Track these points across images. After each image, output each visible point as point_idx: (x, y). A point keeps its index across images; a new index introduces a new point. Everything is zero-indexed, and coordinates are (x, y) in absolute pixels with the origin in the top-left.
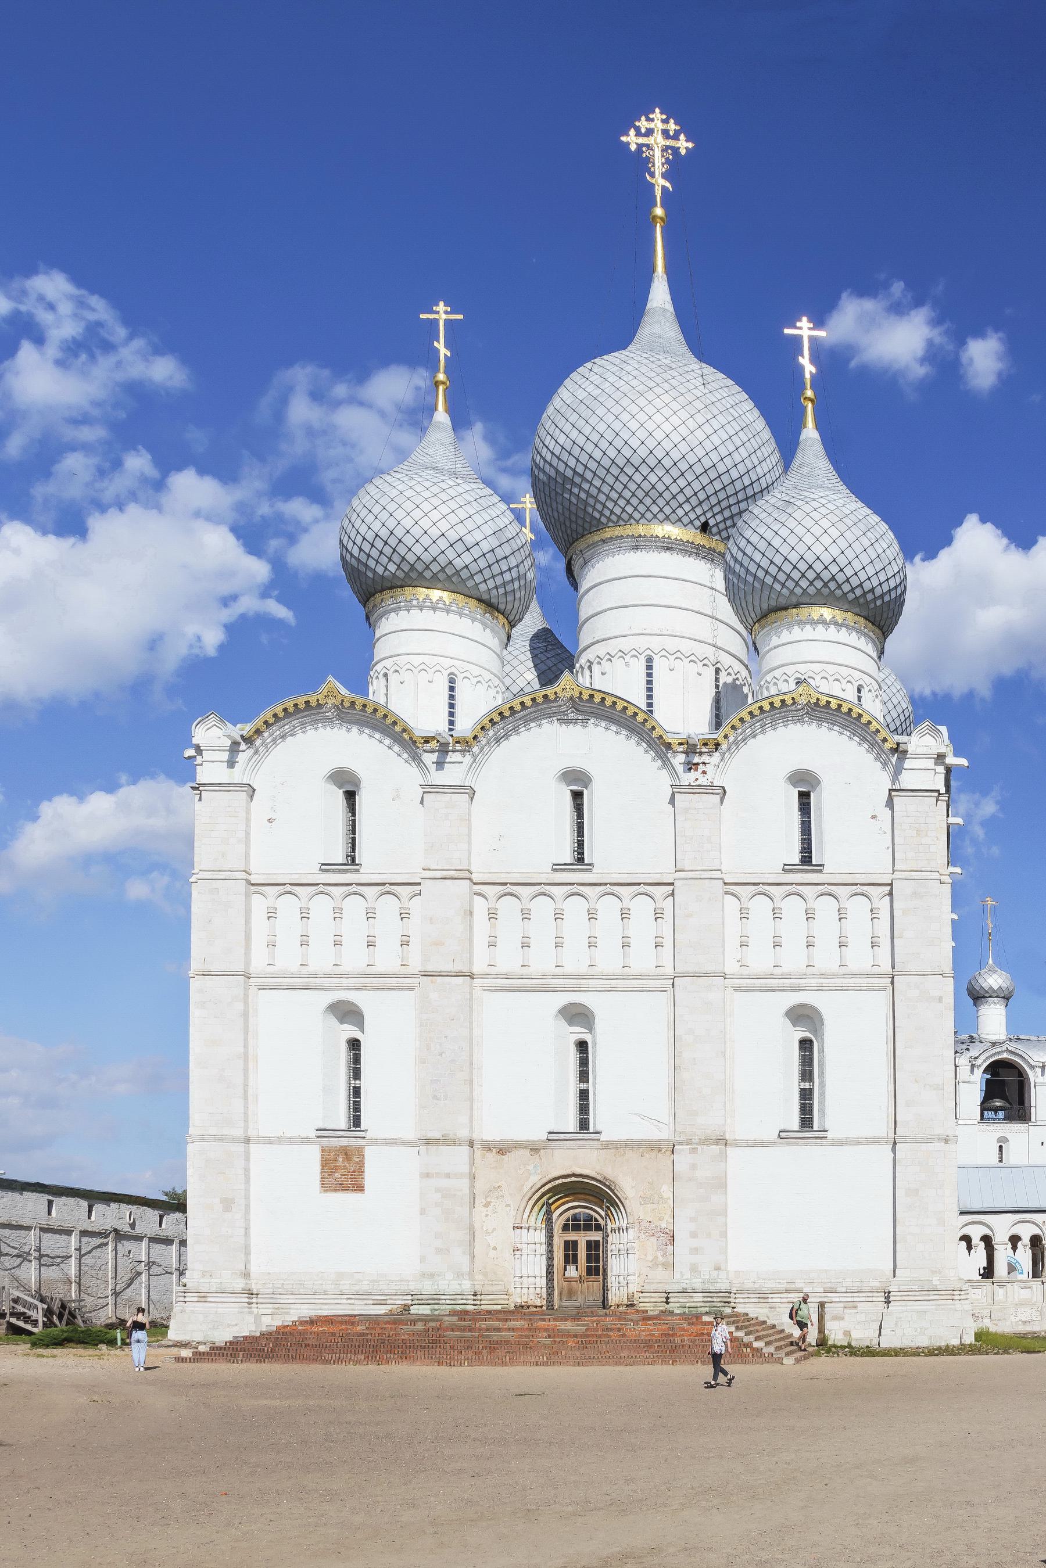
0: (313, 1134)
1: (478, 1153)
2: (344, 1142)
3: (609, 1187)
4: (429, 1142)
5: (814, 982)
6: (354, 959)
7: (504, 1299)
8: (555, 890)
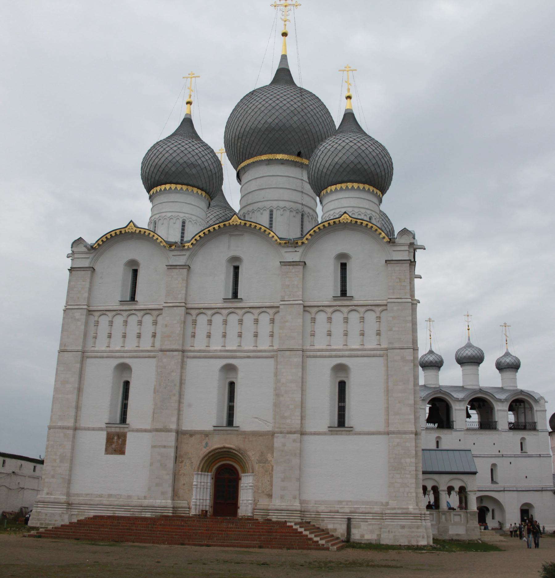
0: (104, 426)
1: (180, 435)
2: (118, 430)
3: (242, 454)
4: (157, 430)
5: (347, 353)
6: (131, 344)
7: (187, 511)
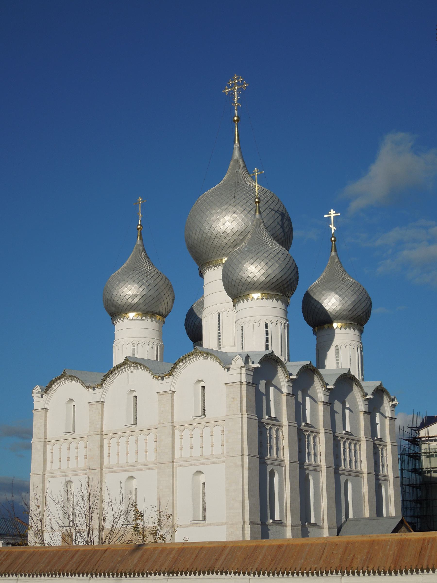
6: (73, 464)
8: (126, 434)
